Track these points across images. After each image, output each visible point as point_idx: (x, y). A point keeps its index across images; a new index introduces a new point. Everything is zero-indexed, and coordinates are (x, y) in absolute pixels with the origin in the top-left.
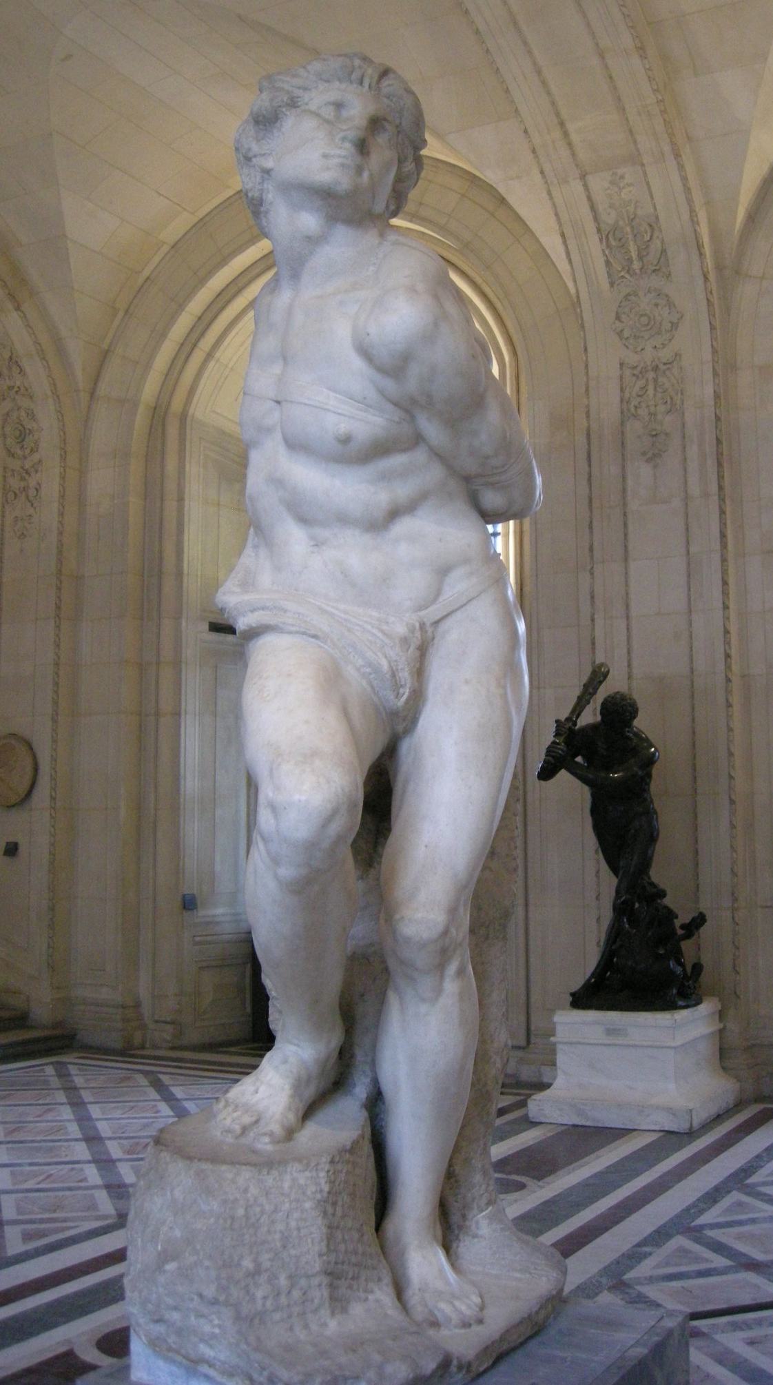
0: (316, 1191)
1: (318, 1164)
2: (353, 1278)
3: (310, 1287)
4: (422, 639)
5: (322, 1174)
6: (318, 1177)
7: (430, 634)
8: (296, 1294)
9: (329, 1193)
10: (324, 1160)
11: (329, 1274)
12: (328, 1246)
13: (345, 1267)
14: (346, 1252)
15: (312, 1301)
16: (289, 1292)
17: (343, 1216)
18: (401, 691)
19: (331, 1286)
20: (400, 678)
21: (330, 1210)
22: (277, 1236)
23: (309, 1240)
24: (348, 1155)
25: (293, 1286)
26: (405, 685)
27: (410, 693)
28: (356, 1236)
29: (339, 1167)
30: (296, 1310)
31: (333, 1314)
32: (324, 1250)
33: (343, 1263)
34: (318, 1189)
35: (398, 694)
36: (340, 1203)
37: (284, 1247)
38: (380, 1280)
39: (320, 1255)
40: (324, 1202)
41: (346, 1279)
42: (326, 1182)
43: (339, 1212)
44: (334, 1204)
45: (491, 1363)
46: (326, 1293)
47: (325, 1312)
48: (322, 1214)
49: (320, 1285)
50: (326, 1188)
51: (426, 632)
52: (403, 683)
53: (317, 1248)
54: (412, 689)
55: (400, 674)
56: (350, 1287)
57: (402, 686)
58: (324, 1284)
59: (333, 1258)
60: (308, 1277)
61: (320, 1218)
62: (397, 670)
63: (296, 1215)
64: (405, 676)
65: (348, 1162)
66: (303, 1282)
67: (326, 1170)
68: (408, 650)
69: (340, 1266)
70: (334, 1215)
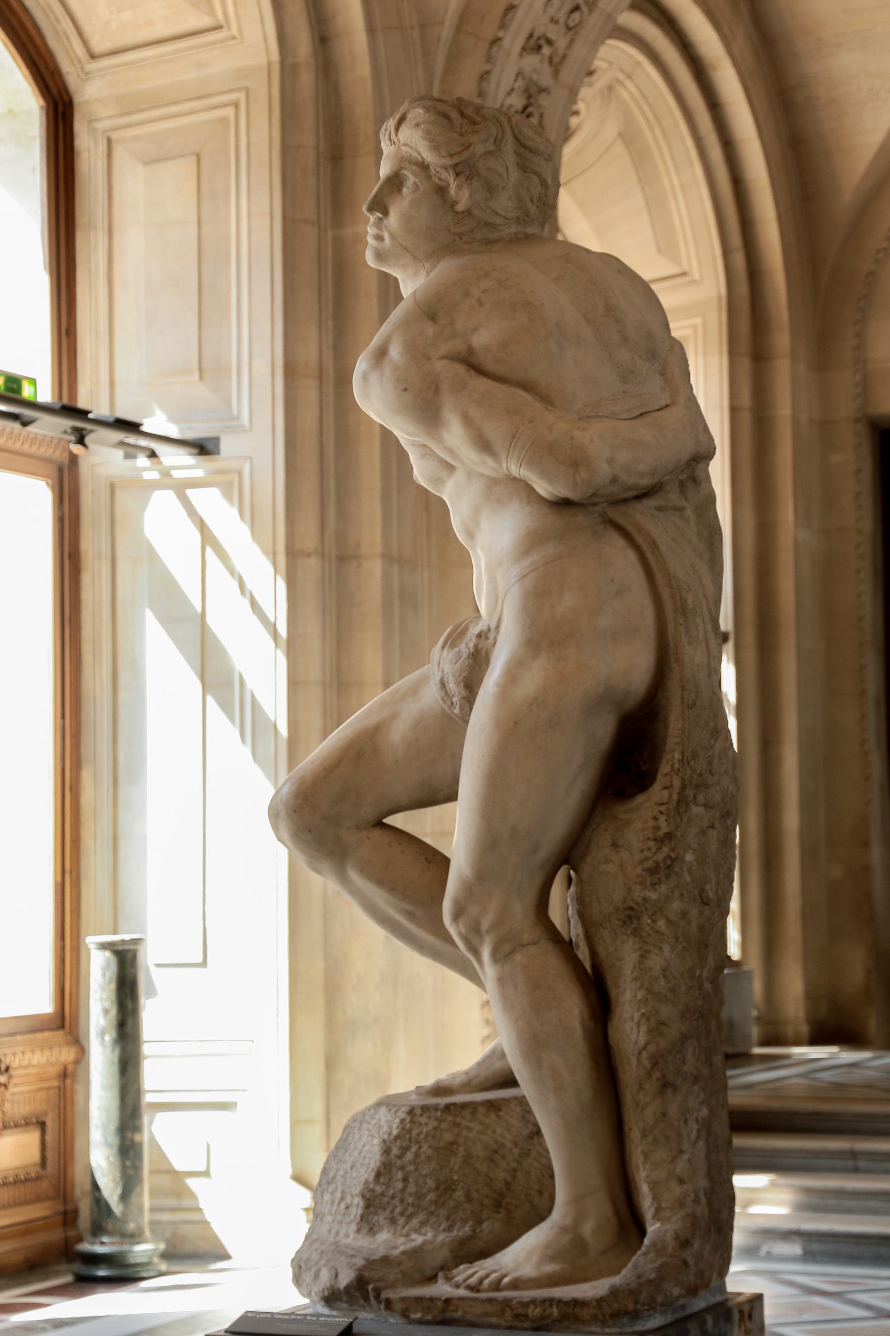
0: (386, 1132)
1: (396, 1112)
2: (402, 1214)
3: (352, 1204)
4: (476, 646)
5: (397, 1121)
6: (394, 1122)
7: (491, 640)
8: (343, 1205)
9: (397, 1137)
10: (404, 1109)
11: (363, 1196)
12: (378, 1175)
13: (396, 1202)
14: (403, 1190)
15: (350, 1216)
16: (339, 1204)
17: (414, 1162)
18: (454, 700)
19: (368, 1206)
20: (450, 688)
21: (395, 1151)
22: (352, 1159)
23: (365, 1168)
24: (439, 1114)
25: (342, 1199)
26: (455, 693)
27: (460, 700)
28: (431, 1183)
29: (423, 1120)
30: (339, 1218)
31: (358, 1231)
32: (372, 1178)
33: (393, 1197)
34: (389, 1131)
35: (452, 703)
36: (414, 1149)
37: (352, 1168)
38: (449, 1229)
39: (366, 1182)
40: (390, 1142)
41: (392, 1212)
42: (398, 1128)
43: (409, 1156)
44: (405, 1149)
45: (429, 1317)
46: (360, 1211)
47: (354, 1227)
48: (382, 1151)
49: (358, 1205)
50: (395, 1132)
51: (487, 638)
52: (453, 693)
53: (366, 1176)
54: (460, 698)
55: (451, 686)
56: (393, 1221)
57: (453, 696)
58: (360, 1206)
59: (379, 1189)
60: (352, 1196)
61: (379, 1154)
62: (448, 682)
63: (367, 1147)
64: (452, 686)
65: (440, 1120)
66: (348, 1199)
67: (402, 1117)
68: (457, 662)
69: (386, 1199)
70: (400, 1157)
